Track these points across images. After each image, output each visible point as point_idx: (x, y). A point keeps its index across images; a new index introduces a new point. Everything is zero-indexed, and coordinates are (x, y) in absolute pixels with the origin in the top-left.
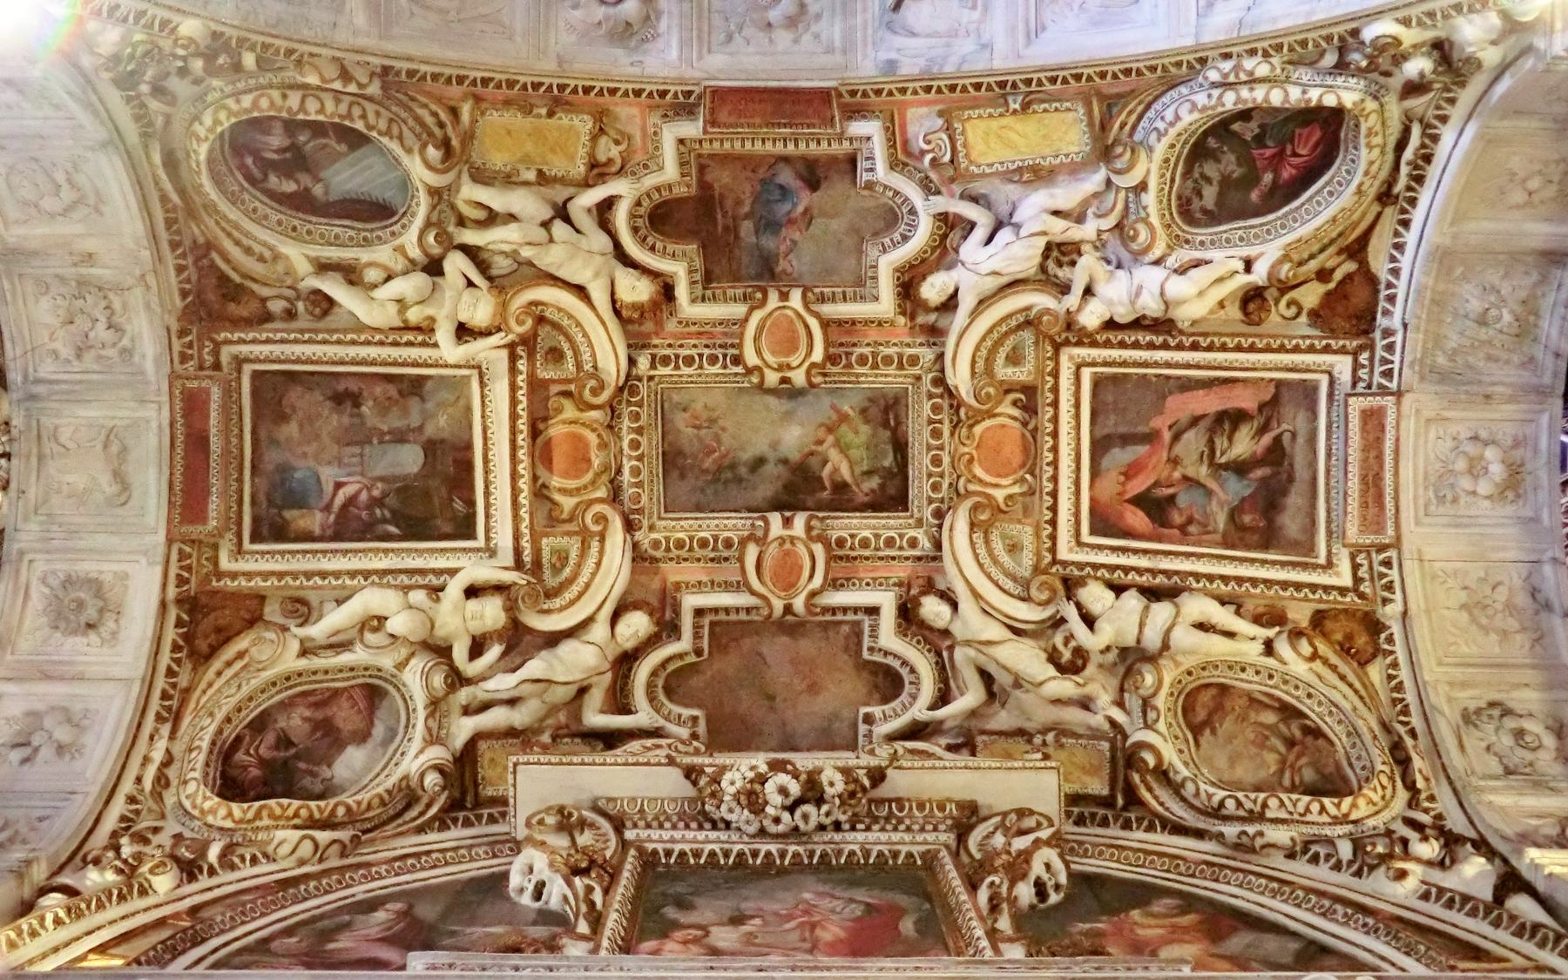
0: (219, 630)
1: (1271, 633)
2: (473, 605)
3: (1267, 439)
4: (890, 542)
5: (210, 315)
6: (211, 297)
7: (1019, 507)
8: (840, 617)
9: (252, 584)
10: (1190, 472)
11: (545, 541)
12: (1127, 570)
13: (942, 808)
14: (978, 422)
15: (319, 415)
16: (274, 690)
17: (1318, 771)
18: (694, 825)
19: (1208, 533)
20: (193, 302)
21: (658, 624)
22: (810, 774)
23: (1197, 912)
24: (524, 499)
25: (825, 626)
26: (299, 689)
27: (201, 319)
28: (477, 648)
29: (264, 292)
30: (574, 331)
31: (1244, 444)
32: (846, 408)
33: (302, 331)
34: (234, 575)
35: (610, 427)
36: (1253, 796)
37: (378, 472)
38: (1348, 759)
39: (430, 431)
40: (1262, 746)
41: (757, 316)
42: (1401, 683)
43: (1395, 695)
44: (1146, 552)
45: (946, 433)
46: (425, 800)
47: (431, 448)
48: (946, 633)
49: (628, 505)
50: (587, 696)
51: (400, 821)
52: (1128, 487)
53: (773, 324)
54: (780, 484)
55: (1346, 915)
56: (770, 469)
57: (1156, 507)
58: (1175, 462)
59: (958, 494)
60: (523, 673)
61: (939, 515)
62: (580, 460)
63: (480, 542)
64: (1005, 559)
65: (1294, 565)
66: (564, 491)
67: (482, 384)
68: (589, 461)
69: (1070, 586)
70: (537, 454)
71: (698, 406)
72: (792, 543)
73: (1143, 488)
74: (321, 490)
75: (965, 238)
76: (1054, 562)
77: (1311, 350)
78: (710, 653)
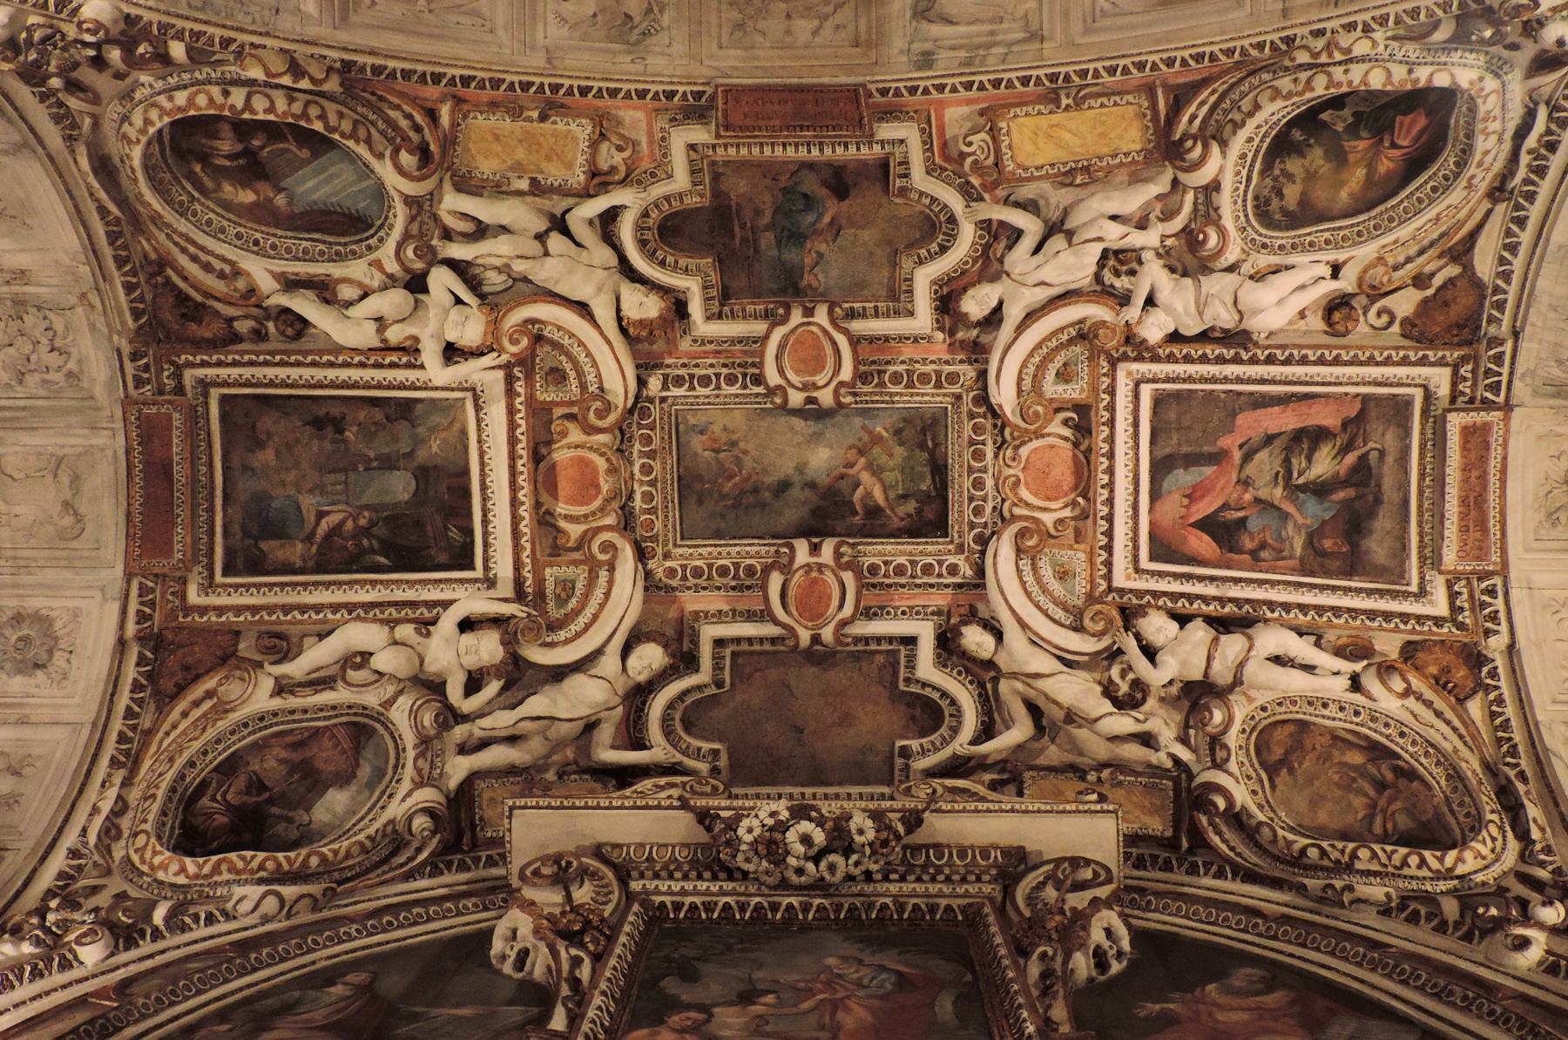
0: (187, 668)
1: (1358, 667)
2: (468, 639)
3: (1351, 458)
4: (927, 570)
5: (167, 337)
6: (168, 316)
7: (1070, 533)
8: (873, 647)
9: (223, 619)
10: (1263, 494)
11: (548, 571)
12: (1191, 598)
13: (985, 856)
14: (1024, 443)
15: (297, 441)
16: (246, 732)
17: (1413, 818)
19: (1284, 558)
20: (149, 322)
21: (673, 655)
22: (837, 820)
23: (1285, 986)
24: (524, 527)
25: (857, 657)
26: (275, 729)
27: (159, 341)
28: (473, 684)
29: (230, 311)
30: (576, 350)
31: (1323, 464)
32: (879, 429)
33: (273, 353)
34: (203, 610)
35: (619, 450)
36: (1340, 845)
37: (363, 501)
38: (1449, 805)
39: (421, 455)
40: (1348, 789)
41: (778, 334)
42: (1508, 720)
43: (1500, 734)
44: (1212, 579)
45: (990, 454)
46: (415, 844)
47: (424, 474)
48: (990, 664)
49: (640, 532)
50: (595, 732)
51: (385, 868)
52: (1194, 509)
53: (797, 341)
54: (807, 508)
55: (1465, 998)
56: (795, 492)
57: (1223, 530)
58: (1245, 483)
59: (1003, 519)
60: (523, 710)
61: (983, 541)
62: (588, 486)
63: (478, 573)
64: (1055, 586)
65: (1381, 593)
66: (567, 518)
67: (478, 408)
68: (598, 487)
69: (1129, 615)
70: (540, 479)
71: (717, 428)
72: (821, 572)
73: (1209, 512)
74: (303, 521)
75: (1010, 248)
76: (1110, 589)
77: (1405, 362)
78: (732, 684)
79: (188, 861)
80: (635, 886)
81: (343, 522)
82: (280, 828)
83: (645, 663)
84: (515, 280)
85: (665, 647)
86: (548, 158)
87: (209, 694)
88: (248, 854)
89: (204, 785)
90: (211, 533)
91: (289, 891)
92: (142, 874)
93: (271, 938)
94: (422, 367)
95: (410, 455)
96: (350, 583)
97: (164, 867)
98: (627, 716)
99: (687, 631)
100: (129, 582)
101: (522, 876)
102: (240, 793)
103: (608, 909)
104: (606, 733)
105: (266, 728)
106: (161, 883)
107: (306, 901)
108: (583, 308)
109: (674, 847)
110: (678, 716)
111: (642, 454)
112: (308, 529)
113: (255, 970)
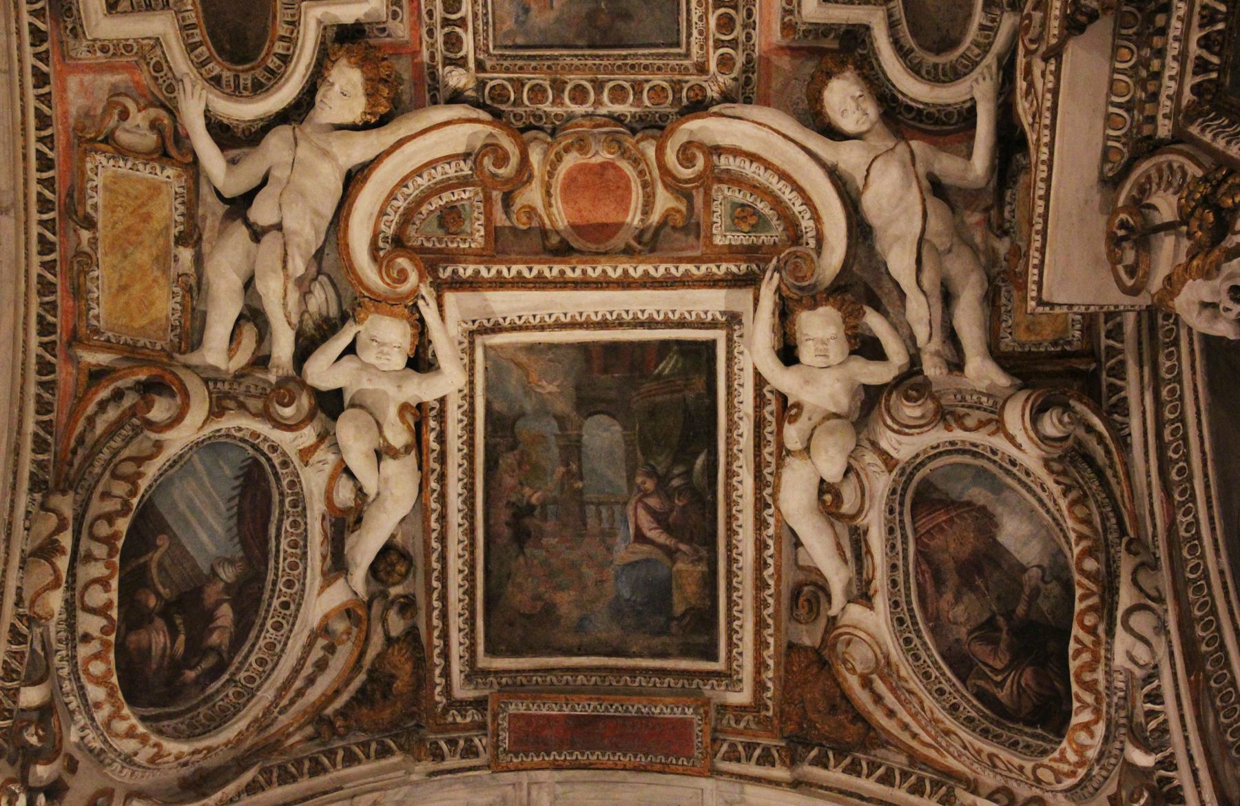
0: (833, 709)
2: (807, 354)
5: (412, 716)
9: (771, 662)
11: (718, 241)
16: (916, 641)
18: (1160, 20)
20: (395, 737)
21: (842, 65)
26: (915, 605)
27: (419, 726)
28: (869, 348)
29: (377, 642)
30: (412, 190)
33: (429, 590)
34: (759, 686)
35: (553, 133)
37: (623, 483)
39: (562, 406)
46: (1081, 432)
47: (587, 404)
50: (946, 181)
51: (1109, 473)
60: (906, 278)
66: (646, 212)
67: (497, 329)
68: (604, 166)
70: (593, 247)
74: (647, 560)
79: (1075, 720)
80: (1164, 129)
81: (648, 509)
82: (1044, 605)
83: (851, 105)
84: (319, 272)
85: (829, 75)
86: (147, 218)
87: (866, 683)
88: (1073, 646)
89: (981, 695)
90: (662, 672)
91: (1126, 597)
92: (1088, 775)
93: (1185, 624)
94: (442, 401)
95: (561, 420)
96: (729, 503)
97: (1081, 749)
98: (925, 135)
99: (810, 42)
100: (721, 773)
101: (1134, 291)
102: (996, 654)
103: (1194, 171)
104: (948, 166)
105: (913, 617)
106: (1101, 754)
107: (1142, 578)
108: (354, 179)
109: (1115, 71)
110: (932, 59)
111: (558, 100)
112: (658, 554)
113: (1222, 647)
